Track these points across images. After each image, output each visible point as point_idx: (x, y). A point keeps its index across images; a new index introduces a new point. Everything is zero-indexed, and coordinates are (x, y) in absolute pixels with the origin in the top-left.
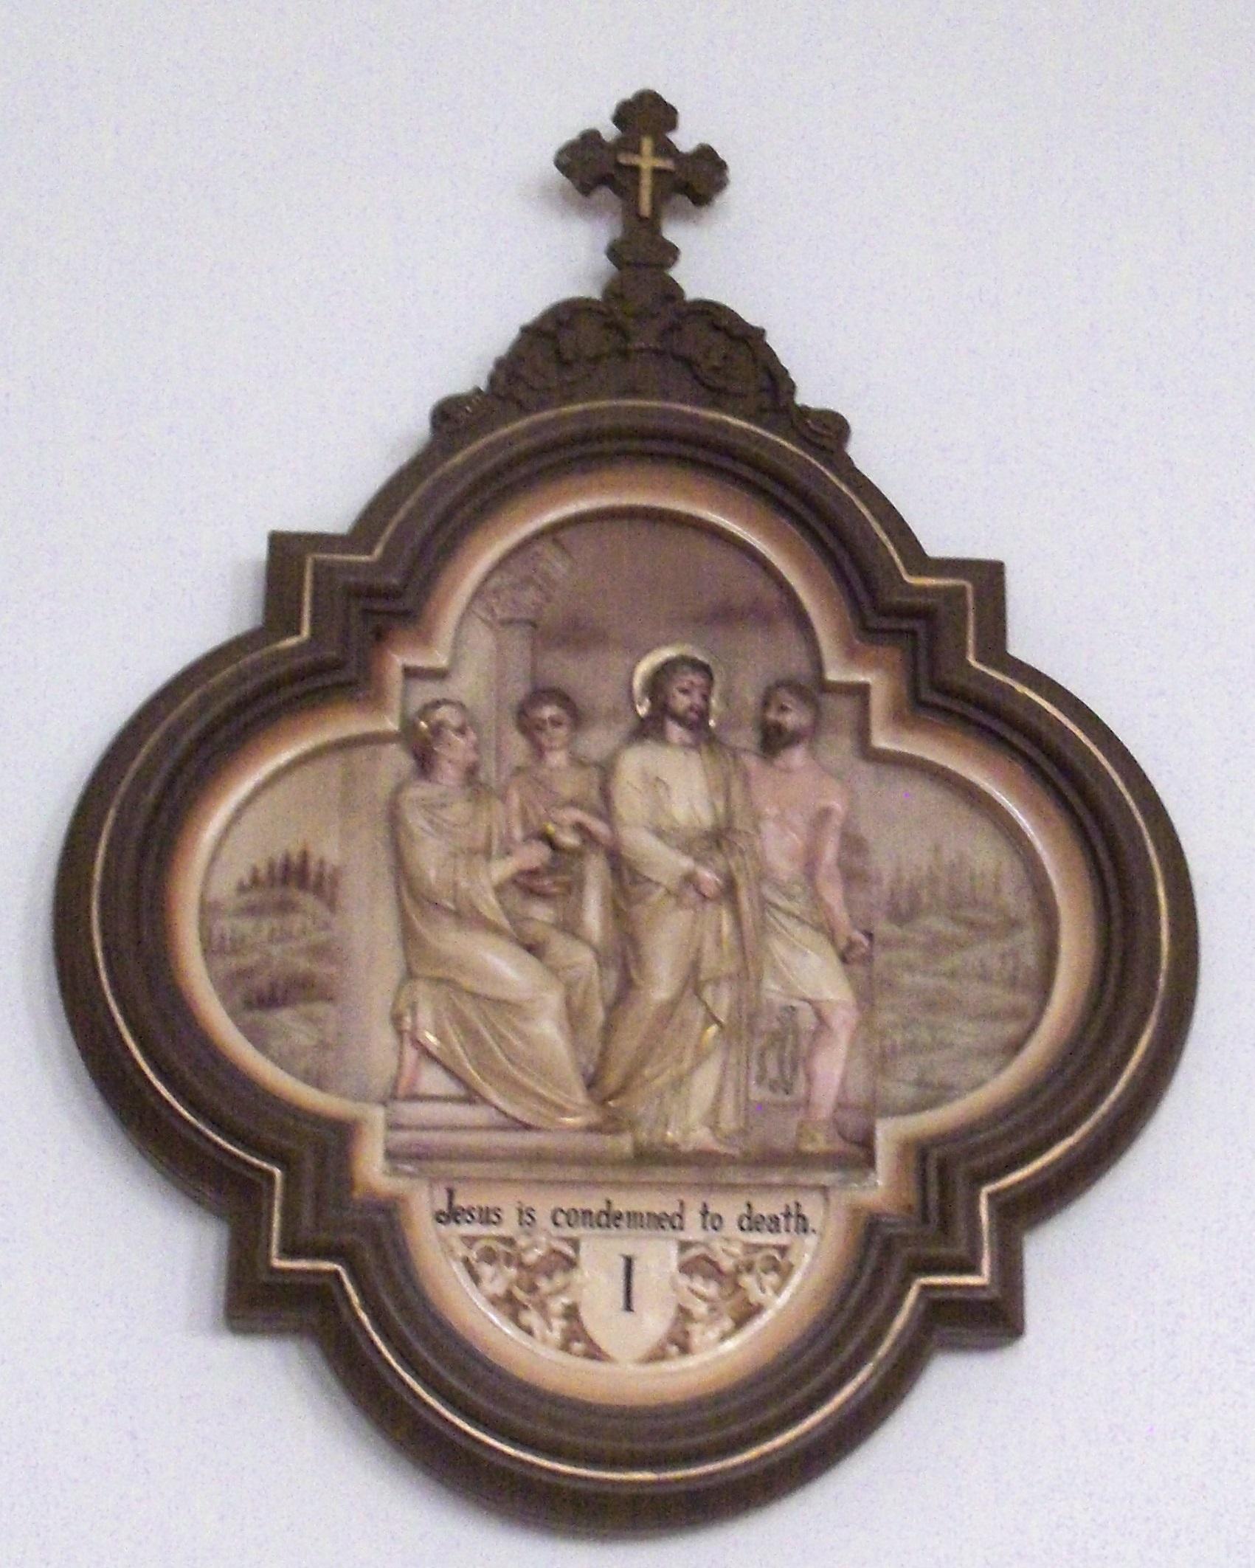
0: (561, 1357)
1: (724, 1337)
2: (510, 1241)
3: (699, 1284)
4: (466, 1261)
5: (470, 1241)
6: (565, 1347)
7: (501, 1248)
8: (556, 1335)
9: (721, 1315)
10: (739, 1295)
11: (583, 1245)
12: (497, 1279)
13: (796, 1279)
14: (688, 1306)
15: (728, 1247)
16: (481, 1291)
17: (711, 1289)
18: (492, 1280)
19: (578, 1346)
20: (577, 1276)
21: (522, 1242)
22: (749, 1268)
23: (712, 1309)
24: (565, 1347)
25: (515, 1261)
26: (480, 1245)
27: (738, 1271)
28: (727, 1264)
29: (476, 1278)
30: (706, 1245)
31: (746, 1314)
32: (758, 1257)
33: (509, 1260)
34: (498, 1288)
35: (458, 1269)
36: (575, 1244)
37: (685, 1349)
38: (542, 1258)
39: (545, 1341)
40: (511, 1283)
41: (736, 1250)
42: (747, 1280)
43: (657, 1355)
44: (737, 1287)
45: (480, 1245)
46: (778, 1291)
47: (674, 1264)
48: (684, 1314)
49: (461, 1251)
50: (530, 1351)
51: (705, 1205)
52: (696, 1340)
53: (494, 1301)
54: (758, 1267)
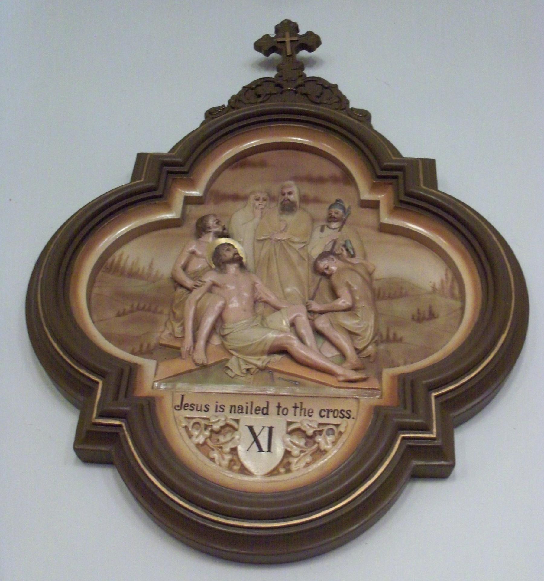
1: (308, 464)
6: (230, 468)
7: (203, 422)
8: (225, 463)
10: (316, 445)
13: (344, 437)
14: (289, 449)
16: (192, 442)
18: (197, 437)
19: (236, 468)
22: (320, 432)
23: (302, 451)
27: (315, 434)
28: (310, 432)
29: (190, 436)
30: (301, 422)
32: (326, 428)
34: (201, 440)
35: (183, 431)
36: (237, 421)
37: (288, 471)
38: (222, 428)
40: (206, 439)
42: (319, 439)
43: (274, 472)
44: (315, 442)
45: (193, 421)
47: (284, 432)
48: (287, 453)
50: (214, 469)
51: (279, 404)
52: (293, 467)
54: (324, 432)
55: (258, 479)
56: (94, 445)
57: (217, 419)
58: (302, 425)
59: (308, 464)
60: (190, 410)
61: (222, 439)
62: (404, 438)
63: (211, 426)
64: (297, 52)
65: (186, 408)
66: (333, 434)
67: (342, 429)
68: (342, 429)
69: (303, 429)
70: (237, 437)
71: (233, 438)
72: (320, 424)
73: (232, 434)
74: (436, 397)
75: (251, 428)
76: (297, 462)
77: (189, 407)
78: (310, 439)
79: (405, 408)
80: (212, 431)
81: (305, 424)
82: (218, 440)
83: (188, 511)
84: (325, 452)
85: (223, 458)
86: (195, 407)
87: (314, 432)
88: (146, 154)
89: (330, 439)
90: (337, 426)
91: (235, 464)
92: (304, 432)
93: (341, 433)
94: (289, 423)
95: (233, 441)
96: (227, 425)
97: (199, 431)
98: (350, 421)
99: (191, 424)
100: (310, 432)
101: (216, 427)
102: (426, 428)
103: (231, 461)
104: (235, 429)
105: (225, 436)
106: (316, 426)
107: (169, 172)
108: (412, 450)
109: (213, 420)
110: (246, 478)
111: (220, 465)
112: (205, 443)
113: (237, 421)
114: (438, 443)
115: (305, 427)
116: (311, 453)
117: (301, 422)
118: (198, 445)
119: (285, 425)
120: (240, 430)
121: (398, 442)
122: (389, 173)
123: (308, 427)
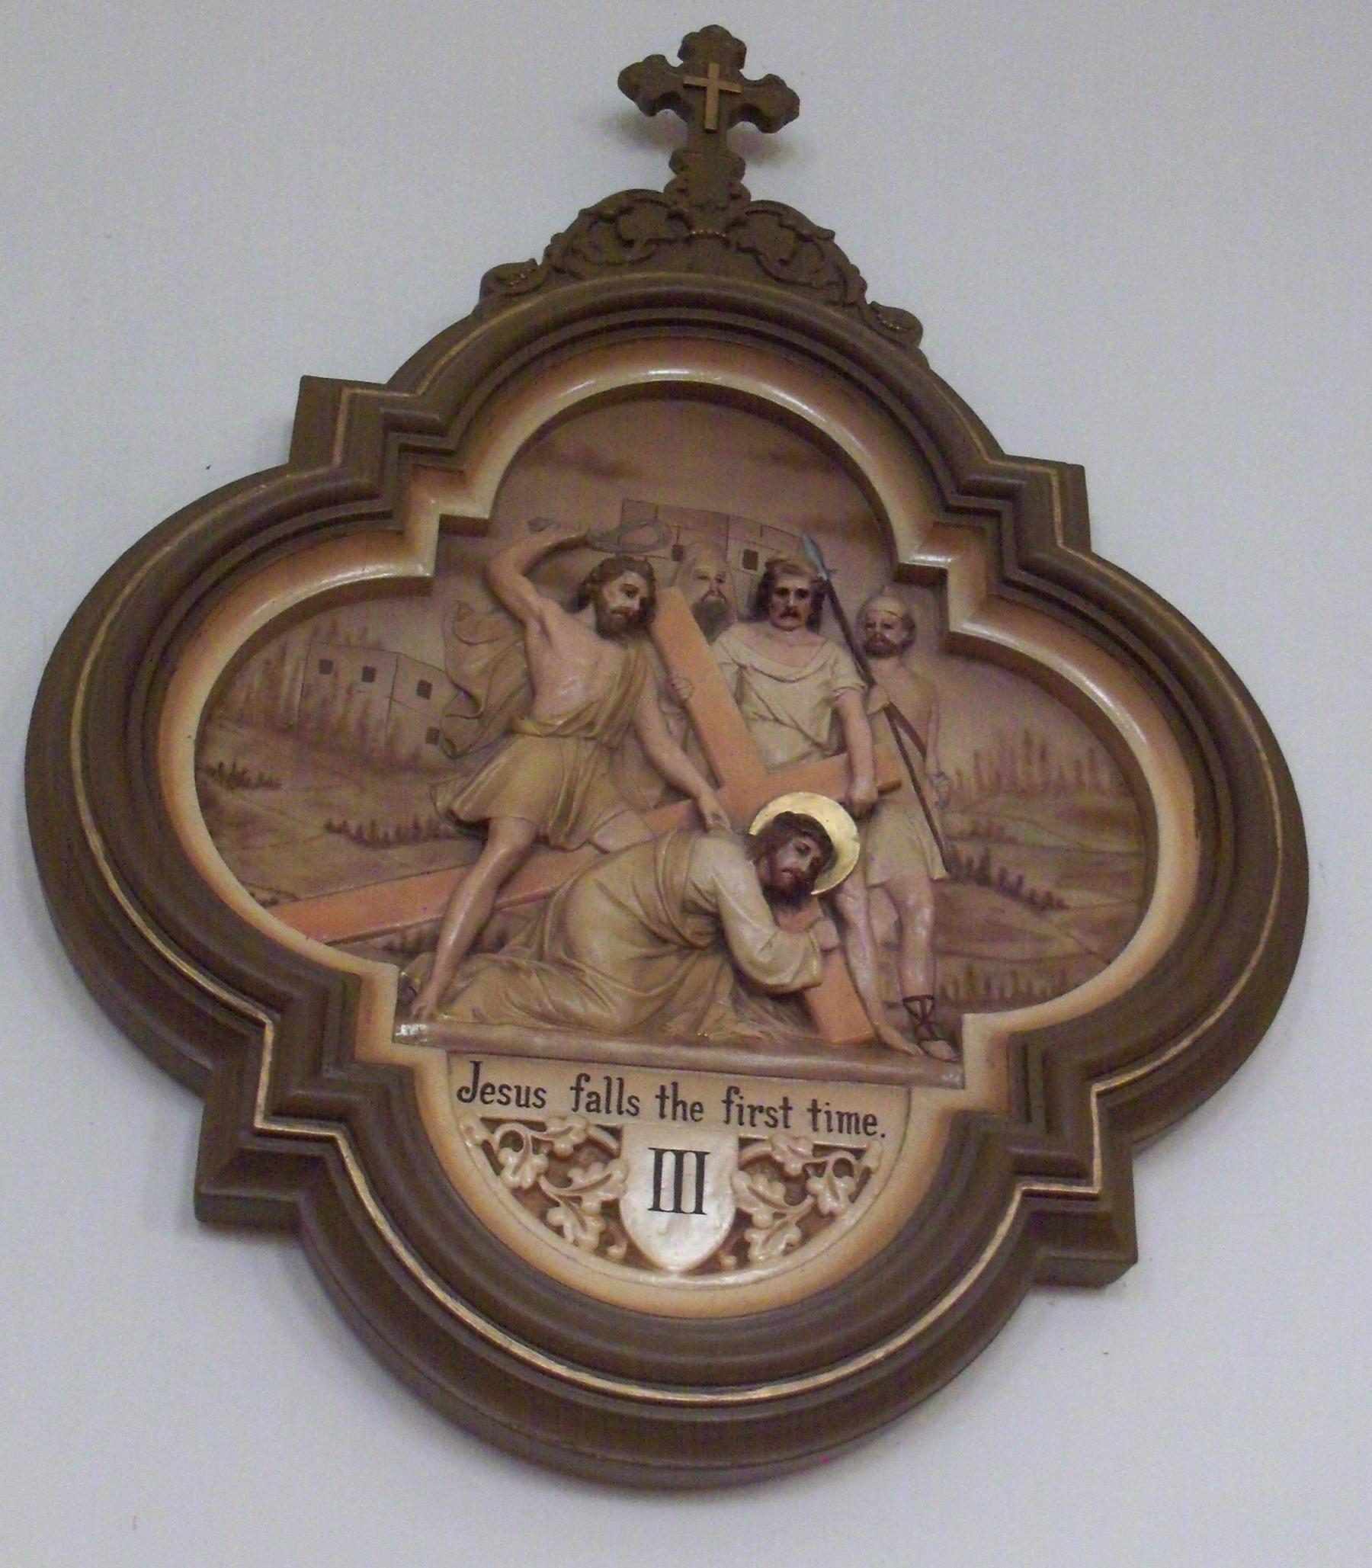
0: (597, 1264)
2: (540, 1126)
4: (486, 1146)
5: (492, 1124)
6: (601, 1250)
7: (527, 1134)
8: (590, 1238)
9: (785, 1225)
11: (626, 1138)
13: (875, 1181)
17: (778, 1192)
19: (616, 1251)
20: (616, 1170)
21: (553, 1128)
22: (819, 1169)
23: (777, 1216)
24: (601, 1250)
25: (545, 1150)
27: (805, 1175)
28: (794, 1167)
29: (498, 1168)
30: (770, 1141)
31: (816, 1221)
32: (832, 1159)
34: (528, 1181)
36: (616, 1133)
38: (577, 1148)
39: (576, 1243)
40: (538, 1175)
41: (804, 1149)
42: (817, 1184)
43: (709, 1266)
44: (805, 1193)
46: (853, 1198)
48: (742, 1220)
49: (481, 1134)
50: (565, 1254)
52: (756, 1252)
54: (829, 1169)
55: (674, 1279)
56: (245, 1188)
57: (567, 1125)
60: (500, 1102)
61: (579, 1178)
62: (1027, 1194)
63: (551, 1143)
64: (732, 123)
65: (488, 1098)
66: (851, 1175)
67: (869, 1161)
68: (869, 1161)
69: (778, 1158)
70: (618, 1175)
71: (608, 1177)
72: (818, 1149)
73: (606, 1163)
76: (767, 1240)
77: (498, 1096)
78: (797, 1186)
79: (1028, 1118)
80: (552, 1155)
81: (784, 1147)
82: (569, 1182)
84: (832, 1216)
85: (583, 1224)
86: (513, 1094)
87: (804, 1170)
88: (338, 385)
89: (844, 1184)
90: (858, 1153)
91: (612, 1243)
92: (779, 1167)
93: (867, 1173)
94: (744, 1143)
96: (590, 1142)
99: (498, 1136)
100: (794, 1167)
103: (602, 1234)
104: (609, 1155)
105: (586, 1168)
107: (404, 449)
110: (643, 1276)
111: (576, 1243)
112: (536, 1187)
113: (616, 1133)
114: (1105, 1207)
115: (782, 1153)
116: (797, 1218)
117: (770, 1141)
118: (518, 1192)
120: (624, 1154)
122: (973, 502)
123: (790, 1155)
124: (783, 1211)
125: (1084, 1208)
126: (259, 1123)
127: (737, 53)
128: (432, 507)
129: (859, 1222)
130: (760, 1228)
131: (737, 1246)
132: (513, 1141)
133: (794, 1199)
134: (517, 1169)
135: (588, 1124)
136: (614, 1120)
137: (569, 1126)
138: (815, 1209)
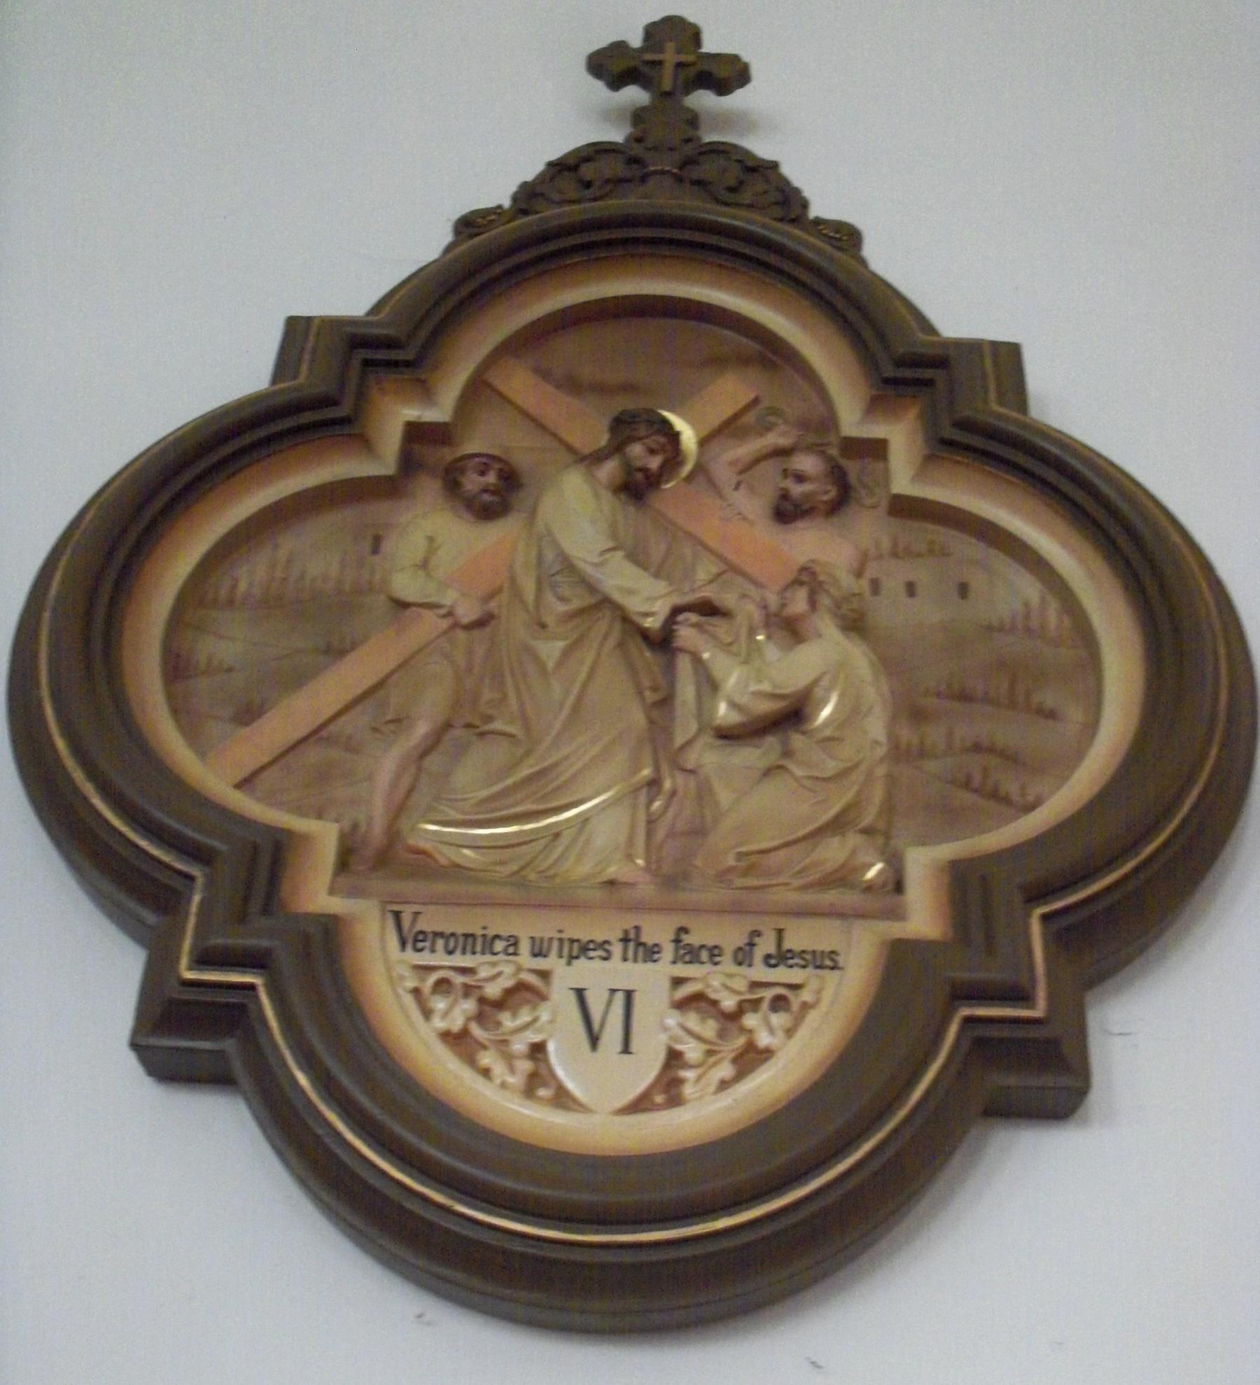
1: (724, 1085)
3: (692, 1020)
4: (416, 992)
7: (459, 980)
12: (459, 1013)
13: (813, 1017)
14: (679, 1047)
15: (723, 983)
17: (709, 1029)
19: (542, 1092)
21: (484, 973)
22: (755, 1004)
23: (710, 1053)
26: (433, 978)
28: (729, 1003)
29: (427, 1013)
30: (704, 979)
31: (751, 1058)
32: (768, 994)
33: (468, 990)
35: (409, 1000)
36: (544, 975)
37: (675, 1100)
38: (509, 992)
40: (469, 1019)
41: (740, 985)
43: (640, 1105)
45: (433, 978)
46: (790, 1032)
48: (674, 1058)
52: (688, 1090)
53: (446, 1036)
54: (765, 1005)
57: (495, 971)
58: (708, 986)
59: (724, 1085)
61: (507, 1021)
63: (479, 987)
65: (420, 945)
67: (806, 996)
69: (713, 996)
70: (545, 1016)
71: (535, 1020)
72: (755, 985)
73: (534, 1008)
74: (1046, 918)
75: (580, 993)
76: (699, 1079)
80: (482, 1001)
82: (499, 1024)
83: (422, 1199)
87: (741, 1003)
89: (778, 1019)
92: (715, 1003)
94: (677, 982)
95: (538, 1024)
97: (451, 998)
98: (831, 977)
100: (729, 1003)
101: (493, 990)
102: (1021, 996)
104: (542, 997)
106: (743, 989)
108: (984, 1047)
109: (484, 973)
111: (503, 1085)
112: (464, 1033)
113: (544, 975)
115: (715, 991)
116: (733, 1055)
118: (446, 1036)
119: (666, 984)
121: (953, 1029)
124: (716, 1048)
125: (1033, 1033)
126: (190, 975)
127: (695, 35)
128: (396, 415)
129: (796, 1055)
130: (692, 1067)
131: (668, 1087)
132: (443, 986)
133: (722, 1034)
134: (446, 1014)
135: (519, 969)
136: (541, 964)
137: (497, 974)
138: (751, 1047)
